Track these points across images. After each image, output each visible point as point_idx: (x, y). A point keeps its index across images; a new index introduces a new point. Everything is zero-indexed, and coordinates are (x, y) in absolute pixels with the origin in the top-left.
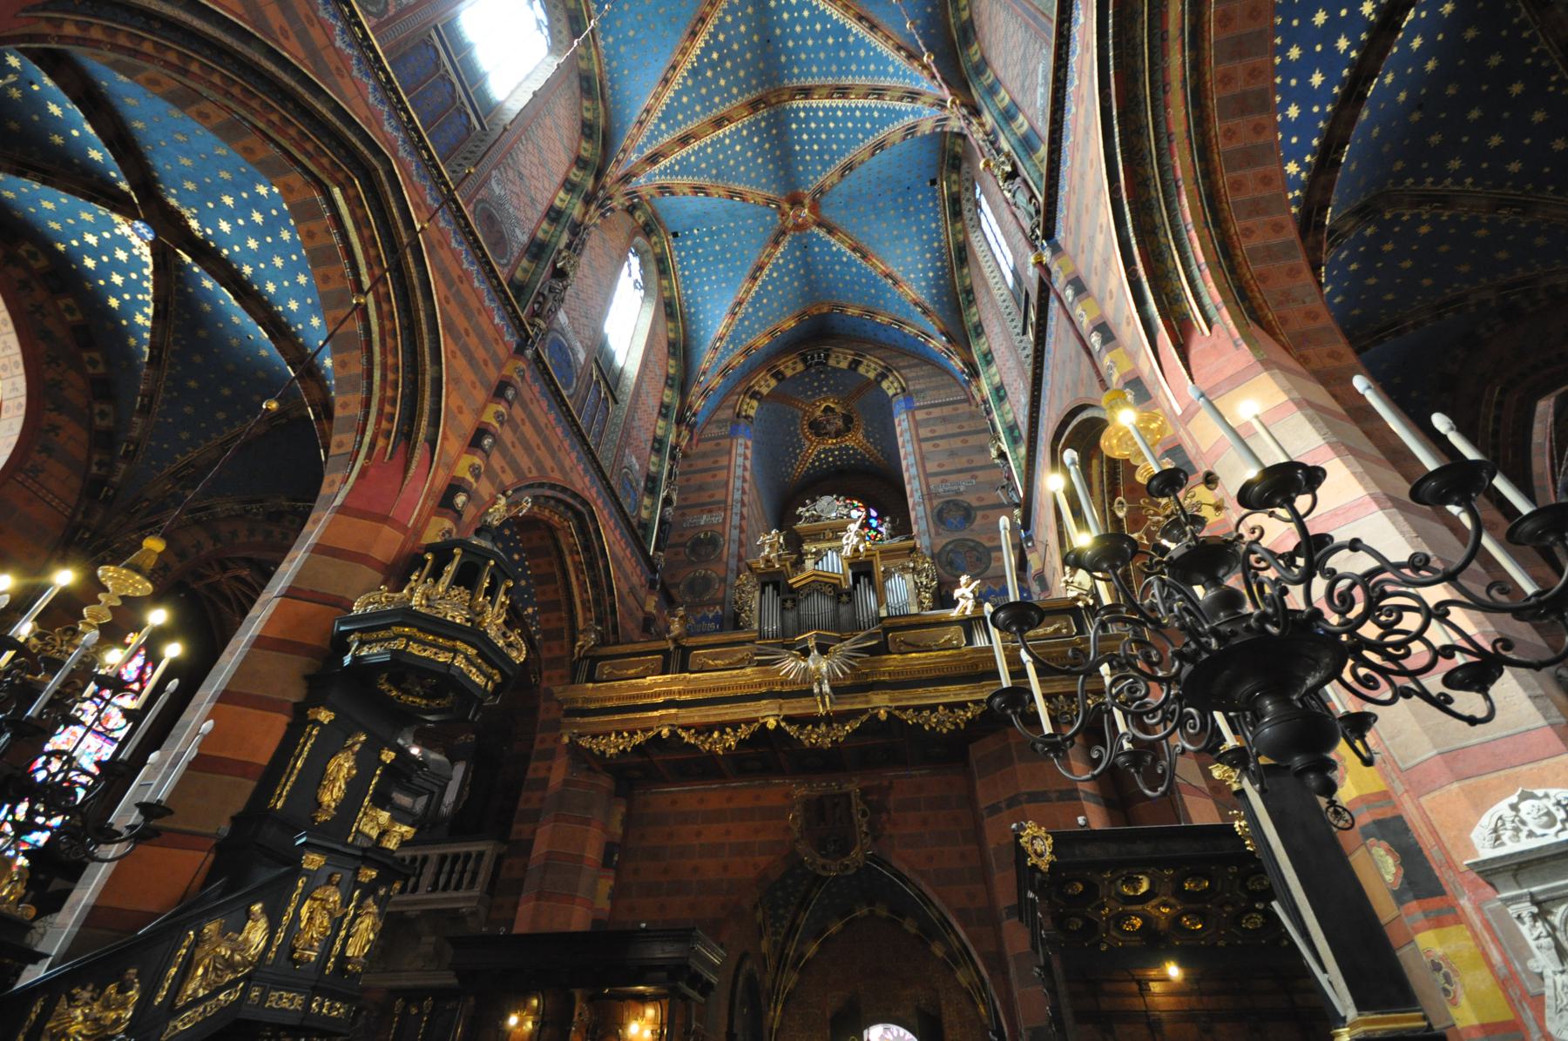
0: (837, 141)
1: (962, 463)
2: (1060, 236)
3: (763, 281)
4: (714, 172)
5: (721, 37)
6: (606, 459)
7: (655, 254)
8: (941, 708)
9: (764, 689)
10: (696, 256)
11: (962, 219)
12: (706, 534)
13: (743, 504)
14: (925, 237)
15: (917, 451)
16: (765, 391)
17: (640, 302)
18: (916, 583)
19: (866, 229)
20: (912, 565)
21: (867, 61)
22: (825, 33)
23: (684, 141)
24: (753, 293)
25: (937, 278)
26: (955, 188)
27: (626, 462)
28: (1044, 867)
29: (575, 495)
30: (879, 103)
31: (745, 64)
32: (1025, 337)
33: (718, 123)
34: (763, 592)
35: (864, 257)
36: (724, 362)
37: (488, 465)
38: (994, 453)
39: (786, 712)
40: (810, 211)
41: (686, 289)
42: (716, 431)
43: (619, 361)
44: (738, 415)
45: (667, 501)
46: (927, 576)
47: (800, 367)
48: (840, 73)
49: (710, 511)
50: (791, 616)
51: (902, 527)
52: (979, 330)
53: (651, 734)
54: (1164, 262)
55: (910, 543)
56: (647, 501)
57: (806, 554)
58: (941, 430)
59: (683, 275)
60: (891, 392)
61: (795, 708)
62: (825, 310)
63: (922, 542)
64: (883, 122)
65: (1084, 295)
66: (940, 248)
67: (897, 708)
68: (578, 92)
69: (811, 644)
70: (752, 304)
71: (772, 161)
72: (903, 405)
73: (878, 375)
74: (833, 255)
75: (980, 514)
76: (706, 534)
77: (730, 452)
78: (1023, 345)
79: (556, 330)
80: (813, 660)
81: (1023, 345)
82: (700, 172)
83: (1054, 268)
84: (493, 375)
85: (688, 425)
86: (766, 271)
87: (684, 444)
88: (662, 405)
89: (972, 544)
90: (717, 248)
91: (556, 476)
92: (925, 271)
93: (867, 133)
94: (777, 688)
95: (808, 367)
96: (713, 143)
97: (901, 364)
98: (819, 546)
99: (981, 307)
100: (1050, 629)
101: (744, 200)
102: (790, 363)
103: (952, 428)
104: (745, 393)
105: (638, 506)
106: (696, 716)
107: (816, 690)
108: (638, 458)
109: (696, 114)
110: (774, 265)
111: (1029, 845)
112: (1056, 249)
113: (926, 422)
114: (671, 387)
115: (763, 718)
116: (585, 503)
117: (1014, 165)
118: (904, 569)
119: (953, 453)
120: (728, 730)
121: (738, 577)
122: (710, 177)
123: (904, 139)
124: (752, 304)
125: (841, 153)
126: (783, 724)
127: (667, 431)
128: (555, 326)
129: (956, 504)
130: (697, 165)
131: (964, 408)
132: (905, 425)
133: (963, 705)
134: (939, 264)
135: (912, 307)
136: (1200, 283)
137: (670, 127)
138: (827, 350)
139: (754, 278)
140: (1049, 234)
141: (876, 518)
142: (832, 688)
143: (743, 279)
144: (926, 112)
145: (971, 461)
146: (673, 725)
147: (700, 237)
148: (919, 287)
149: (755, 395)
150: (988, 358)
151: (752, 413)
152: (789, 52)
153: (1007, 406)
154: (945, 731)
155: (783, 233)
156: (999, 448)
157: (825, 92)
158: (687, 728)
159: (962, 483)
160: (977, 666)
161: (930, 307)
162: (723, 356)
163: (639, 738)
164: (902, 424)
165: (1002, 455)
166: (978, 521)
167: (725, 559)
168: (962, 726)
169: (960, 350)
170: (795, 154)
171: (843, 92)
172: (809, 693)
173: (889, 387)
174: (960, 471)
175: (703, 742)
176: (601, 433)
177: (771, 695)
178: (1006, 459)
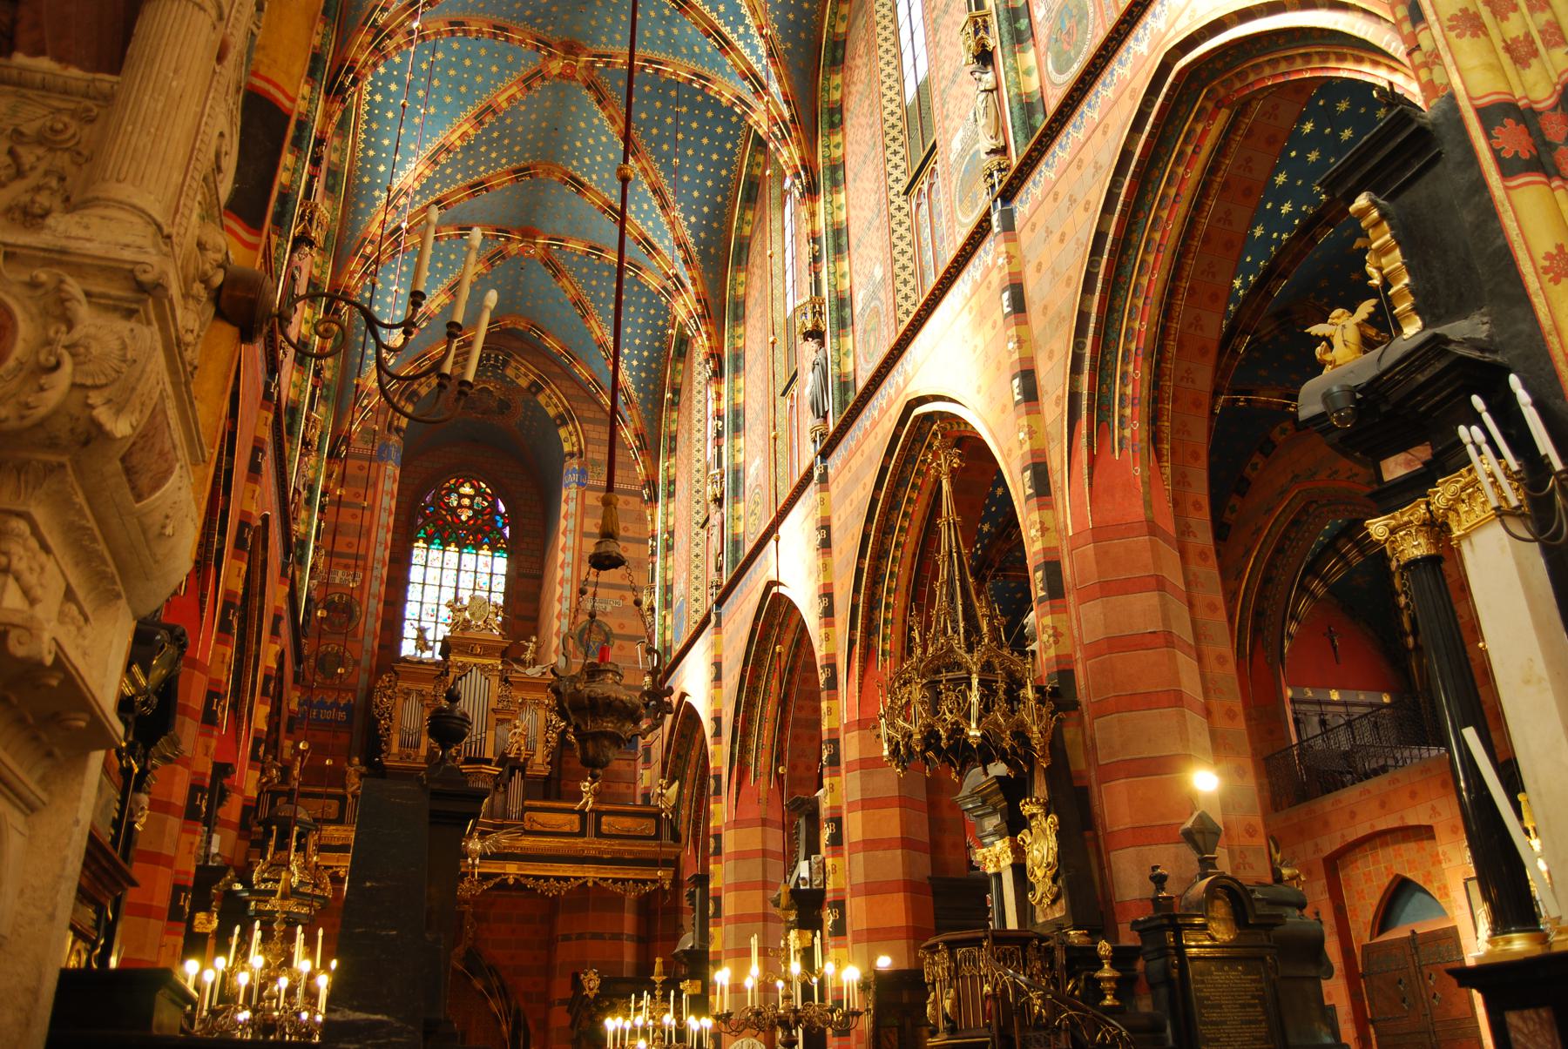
5: (508, 121)
12: (341, 597)
14: (652, 312)
15: (577, 548)
25: (650, 360)
28: (591, 995)
32: (701, 531)
60: (567, 448)
72: (575, 477)
73: (560, 416)
75: (617, 642)
78: (697, 539)
97: (587, 414)
109: (455, 181)
117: (722, 494)
118: (539, 703)
132: (572, 505)
133: (566, 879)
134: (657, 344)
140: (720, 602)
141: (502, 516)
161: (634, 395)
165: (652, 609)
167: (360, 636)
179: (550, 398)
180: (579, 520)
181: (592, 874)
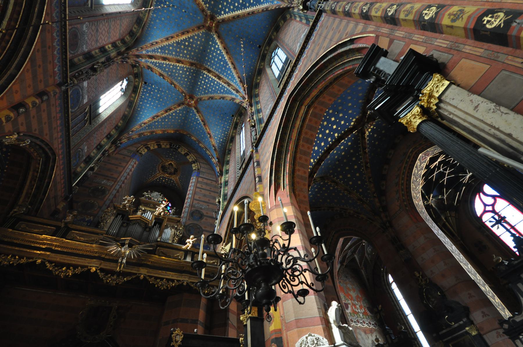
0: (212, 89)
1: (206, 200)
2: (259, 148)
3: (169, 114)
4: (170, 73)
5: (191, 40)
6: (74, 141)
7: (135, 85)
8: (165, 280)
9: (97, 255)
10: (150, 93)
11: (236, 130)
12: (102, 187)
13: (123, 183)
16: (152, 148)
17: (120, 96)
18: (175, 233)
19: (209, 117)
20: (176, 226)
21: (229, 75)
22: (221, 60)
23: (164, 59)
24: (164, 116)
25: (222, 142)
26: (238, 121)
27: (81, 147)
29: (51, 149)
30: (228, 87)
31: (195, 52)
33: (178, 61)
34: (116, 217)
35: (204, 125)
36: (142, 132)
37: (16, 119)
38: (217, 200)
39: (102, 266)
40: (194, 103)
41: (140, 101)
42: (126, 153)
43: (101, 110)
44: (138, 151)
45: (92, 169)
46: (180, 232)
47: (168, 146)
48: (221, 73)
49: (108, 180)
50: (123, 229)
51: (178, 213)
52: (228, 163)
53: (31, 260)
54: (279, 168)
55: (179, 219)
56: (82, 165)
57: (140, 210)
58: (204, 187)
59: (141, 97)
60: (194, 168)
61: (107, 266)
62: (185, 133)
63: (183, 220)
64: (226, 93)
65: (259, 166)
66: (227, 134)
67: (149, 276)
68: (134, 21)
69: (127, 242)
70: (162, 119)
71: (190, 82)
72: (196, 174)
73: (192, 161)
74: (196, 119)
75: (205, 218)
76: (102, 187)
77: (128, 162)
78: (238, 173)
79: (80, 87)
80: (124, 249)
81: (238, 173)
82: (165, 71)
83: (254, 156)
84: (41, 87)
85: (116, 146)
86: (172, 112)
87: (111, 151)
88: (109, 134)
89: (199, 227)
90: (159, 95)
91: (47, 138)
92: (220, 138)
93: (221, 93)
94: (103, 256)
95: (171, 148)
96: (173, 65)
97: (201, 161)
98: (146, 208)
99: (231, 156)
100: (212, 262)
101: (175, 87)
102: (165, 144)
103: (208, 188)
104: (144, 146)
105: (77, 165)
106: (59, 258)
107: (120, 261)
108: (88, 148)
110: (175, 111)
111: (174, 337)
112: (257, 151)
113: (201, 183)
114: (116, 130)
115: (91, 266)
116: (54, 154)
117: (255, 124)
118: (173, 227)
119: (205, 196)
120: (71, 268)
121: (107, 208)
122: (167, 74)
123: (230, 100)
124: (162, 119)
125: (211, 93)
126: (98, 271)
127: (106, 144)
128: (80, 85)
129: (199, 212)
130: (165, 68)
131: (214, 183)
132: (194, 180)
133: (173, 281)
135: (212, 146)
136: (285, 177)
137: (161, 52)
138: (180, 146)
139: (166, 111)
140: (257, 146)
141: (170, 207)
142: (126, 261)
143: (162, 110)
144: (239, 97)
145: (209, 200)
146: (44, 259)
147: (155, 89)
148: (216, 142)
149: (147, 148)
150: (227, 172)
151: (143, 153)
152: (209, 58)
153: (227, 188)
154: (162, 289)
155: (183, 104)
156: (219, 199)
157: (214, 75)
158: (50, 262)
159: (204, 206)
160: (184, 267)
162: (142, 129)
163: (23, 261)
164: (193, 180)
165: (219, 202)
166: (204, 220)
168: (169, 288)
169: (220, 166)
170: (198, 85)
171: (220, 78)
172: (116, 261)
173: (194, 167)
174: (204, 202)
175: (56, 270)
176: (77, 131)
177: (99, 258)
178: (220, 204)
179: (191, 157)
180: (196, 184)
181: (187, 279)
